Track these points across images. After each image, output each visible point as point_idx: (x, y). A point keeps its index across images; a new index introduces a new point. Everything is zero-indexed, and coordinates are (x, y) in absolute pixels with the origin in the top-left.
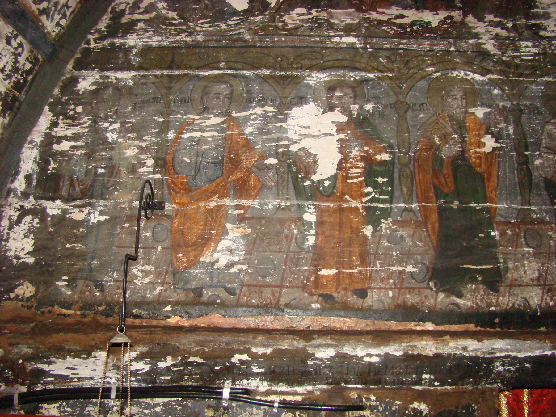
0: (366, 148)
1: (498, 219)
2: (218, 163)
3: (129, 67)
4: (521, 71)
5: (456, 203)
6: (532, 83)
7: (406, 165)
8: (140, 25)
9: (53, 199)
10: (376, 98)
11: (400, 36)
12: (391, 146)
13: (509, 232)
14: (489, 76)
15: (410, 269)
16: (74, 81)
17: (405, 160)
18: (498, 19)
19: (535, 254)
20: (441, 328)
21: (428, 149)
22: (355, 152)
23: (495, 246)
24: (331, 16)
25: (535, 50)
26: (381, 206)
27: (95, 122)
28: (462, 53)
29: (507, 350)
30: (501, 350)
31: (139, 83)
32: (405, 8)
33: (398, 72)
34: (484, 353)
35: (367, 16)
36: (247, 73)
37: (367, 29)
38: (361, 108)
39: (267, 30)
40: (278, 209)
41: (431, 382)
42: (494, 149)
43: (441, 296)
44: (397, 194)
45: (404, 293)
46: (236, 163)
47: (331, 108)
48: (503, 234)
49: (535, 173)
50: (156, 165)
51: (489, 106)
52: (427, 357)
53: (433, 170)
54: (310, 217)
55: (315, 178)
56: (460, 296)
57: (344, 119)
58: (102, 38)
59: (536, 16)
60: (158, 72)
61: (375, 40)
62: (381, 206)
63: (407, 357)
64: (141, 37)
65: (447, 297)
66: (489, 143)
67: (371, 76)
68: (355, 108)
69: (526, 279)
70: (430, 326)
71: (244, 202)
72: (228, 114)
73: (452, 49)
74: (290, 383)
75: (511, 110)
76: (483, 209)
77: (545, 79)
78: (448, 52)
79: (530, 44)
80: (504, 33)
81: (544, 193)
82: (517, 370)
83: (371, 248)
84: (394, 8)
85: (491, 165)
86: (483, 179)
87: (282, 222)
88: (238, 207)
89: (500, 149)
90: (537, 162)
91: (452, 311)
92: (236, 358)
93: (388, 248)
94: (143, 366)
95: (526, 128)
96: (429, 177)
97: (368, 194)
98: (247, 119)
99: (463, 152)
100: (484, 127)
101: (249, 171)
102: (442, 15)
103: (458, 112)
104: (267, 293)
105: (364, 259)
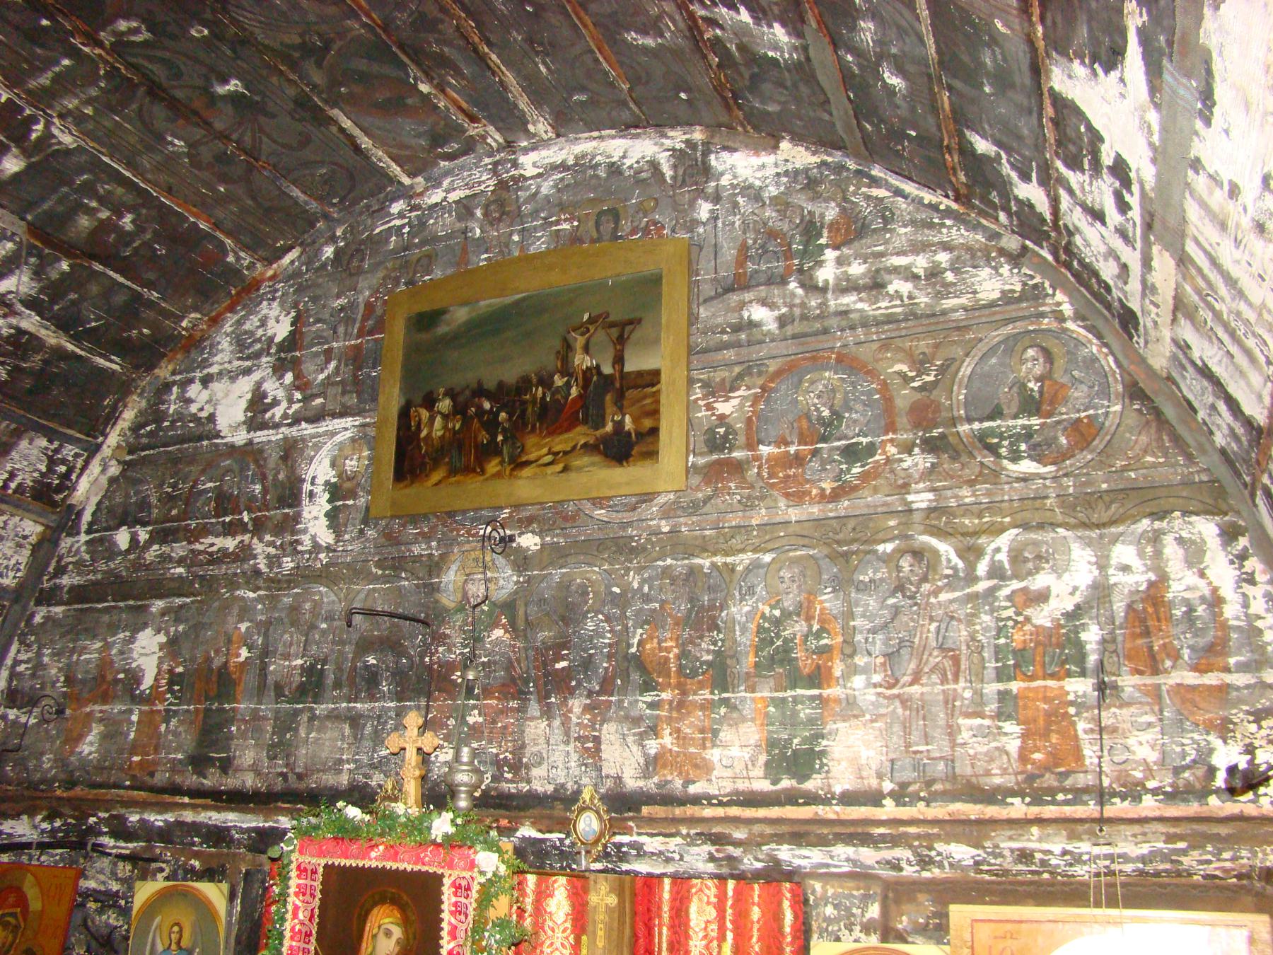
1: (239, 717)
6: (285, 595)
8: (71, 567)
9: (12, 708)
10: (187, 620)
11: (210, 562)
15: (180, 756)
16: (33, 615)
22: (165, 667)
24: (172, 550)
25: (292, 565)
27: (39, 648)
28: (244, 573)
41: (201, 844)
43: (195, 777)
46: (103, 677)
47: (158, 632)
48: (239, 729)
60: (76, 606)
66: (244, 653)
67: (188, 600)
71: (104, 708)
72: (105, 640)
74: (126, 841)
78: (236, 574)
81: (272, 694)
85: (241, 673)
88: (101, 711)
90: (272, 668)
99: (226, 663)
105: (156, 751)
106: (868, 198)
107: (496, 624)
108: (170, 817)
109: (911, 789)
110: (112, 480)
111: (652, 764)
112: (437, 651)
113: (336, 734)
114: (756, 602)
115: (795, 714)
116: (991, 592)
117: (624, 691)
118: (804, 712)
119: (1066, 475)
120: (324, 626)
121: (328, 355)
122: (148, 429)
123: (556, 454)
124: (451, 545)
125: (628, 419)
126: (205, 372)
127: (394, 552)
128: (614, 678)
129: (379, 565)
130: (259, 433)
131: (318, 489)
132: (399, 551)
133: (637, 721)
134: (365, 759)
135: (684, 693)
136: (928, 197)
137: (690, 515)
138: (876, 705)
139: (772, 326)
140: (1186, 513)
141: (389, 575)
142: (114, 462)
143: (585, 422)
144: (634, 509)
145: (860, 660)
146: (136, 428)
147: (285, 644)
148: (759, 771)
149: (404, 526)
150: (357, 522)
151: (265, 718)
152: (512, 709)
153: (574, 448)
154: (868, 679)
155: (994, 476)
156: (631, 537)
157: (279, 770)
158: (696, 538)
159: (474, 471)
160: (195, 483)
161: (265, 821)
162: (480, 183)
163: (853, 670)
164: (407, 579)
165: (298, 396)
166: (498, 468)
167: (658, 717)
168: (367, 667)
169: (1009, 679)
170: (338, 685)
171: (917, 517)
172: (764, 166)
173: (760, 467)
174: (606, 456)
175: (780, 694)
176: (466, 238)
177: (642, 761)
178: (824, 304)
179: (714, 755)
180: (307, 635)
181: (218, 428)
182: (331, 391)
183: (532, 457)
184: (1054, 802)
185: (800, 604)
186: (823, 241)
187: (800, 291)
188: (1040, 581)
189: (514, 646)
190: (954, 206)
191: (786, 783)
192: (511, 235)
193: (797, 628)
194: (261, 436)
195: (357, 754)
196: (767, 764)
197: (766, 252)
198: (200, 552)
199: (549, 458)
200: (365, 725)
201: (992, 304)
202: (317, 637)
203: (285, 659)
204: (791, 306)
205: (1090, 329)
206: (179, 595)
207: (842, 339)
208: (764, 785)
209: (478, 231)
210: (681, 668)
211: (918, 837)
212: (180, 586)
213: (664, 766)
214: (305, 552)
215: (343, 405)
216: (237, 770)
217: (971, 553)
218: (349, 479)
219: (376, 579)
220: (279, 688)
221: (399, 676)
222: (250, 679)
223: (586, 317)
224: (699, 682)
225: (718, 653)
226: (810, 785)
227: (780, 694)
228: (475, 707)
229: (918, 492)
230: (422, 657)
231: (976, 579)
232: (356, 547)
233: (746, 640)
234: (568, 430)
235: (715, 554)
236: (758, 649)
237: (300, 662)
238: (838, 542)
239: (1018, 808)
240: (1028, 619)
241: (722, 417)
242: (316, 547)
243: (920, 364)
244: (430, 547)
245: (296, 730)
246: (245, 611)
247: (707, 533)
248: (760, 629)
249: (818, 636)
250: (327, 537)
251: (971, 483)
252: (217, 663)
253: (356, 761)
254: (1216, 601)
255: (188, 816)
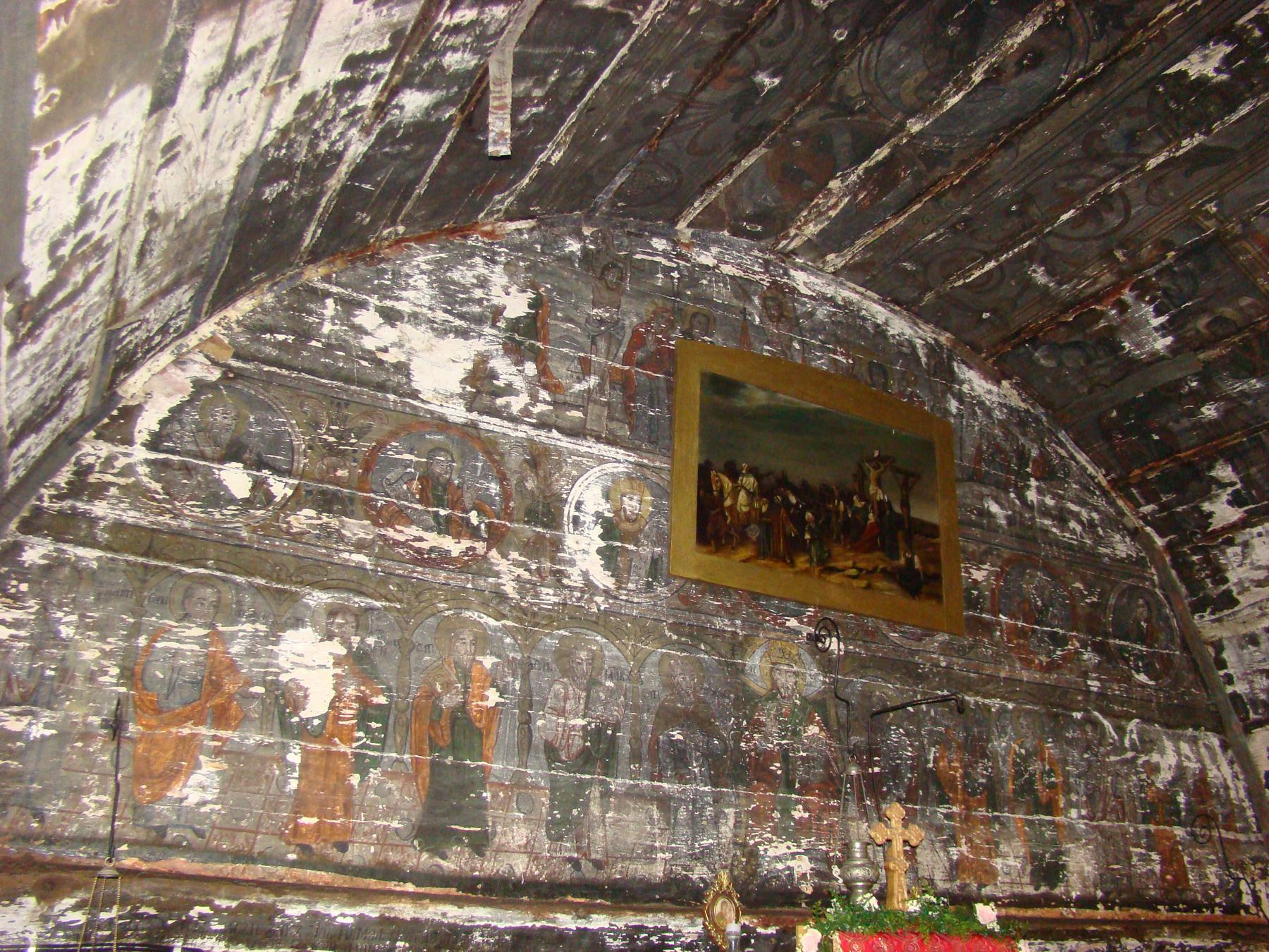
0: (363, 688)
1: (492, 779)
2: (197, 683)
3: (94, 544)
4: (537, 620)
5: (451, 758)
6: (546, 635)
7: (403, 712)
8: (113, 491)
11: (416, 562)
12: (389, 689)
13: (501, 794)
14: (504, 622)
15: (395, 824)
17: (402, 706)
18: (523, 559)
19: (525, 820)
20: (421, 890)
21: (428, 697)
22: (351, 691)
23: (486, 809)
25: (556, 599)
26: (371, 753)
27: (44, 608)
29: (487, 919)
30: (481, 919)
31: (107, 567)
32: (426, 529)
33: (408, 604)
34: (464, 921)
35: (383, 532)
36: (239, 579)
37: (381, 548)
38: (362, 641)
39: (265, 529)
40: (260, 745)
42: (497, 704)
43: (425, 856)
44: (390, 742)
45: (386, 850)
46: (217, 687)
47: (330, 637)
48: (494, 796)
49: (536, 735)
50: (121, 676)
51: (498, 656)
52: (403, 921)
53: (431, 720)
54: (294, 757)
55: (304, 714)
56: (444, 857)
57: (343, 651)
58: (60, 497)
59: (562, 561)
60: (131, 558)
61: (388, 563)
62: (371, 753)
63: (384, 920)
64: (113, 506)
65: (431, 857)
66: (493, 697)
67: (378, 604)
68: (355, 640)
69: (513, 845)
70: (410, 887)
71: (222, 733)
72: (212, 626)
73: (469, 586)
75: (521, 663)
76: (477, 767)
77: (562, 632)
79: (551, 591)
80: (526, 575)
81: (542, 756)
82: (497, 942)
83: (357, 799)
84: (414, 527)
85: (491, 721)
86: (481, 735)
87: (264, 760)
88: (215, 738)
89: (503, 704)
90: (540, 723)
91: (434, 872)
92: (195, 912)
93: (374, 800)
94: (80, 917)
95: (533, 685)
96: (425, 727)
97: (359, 739)
98: (233, 635)
99: (465, 703)
100: (490, 679)
101: (231, 697)
102: (466, 543)
103: (465, 660)
104: (241, 839)
105: (348, 809)
106: (1056, 452)
107: (811, 721)
108: (371, 911)
109: (1112, 896)
110: (200, 386)
111: (956, 868)
112: (753, 738)
113: (642, 816)
114: (1010, 739)
115: (1042, 833)
116: (1134, 759)
117: (924, 801)
118: (1048, 834)
119: (1161, 689)
120: (609, 684)
121: (586, 367)
122: (281, 337)
123: (860, 570)
124: (757, 628)
125: (916, 559)
126: (389, 303)
127: (692, 619)
128: (916, 788)
129: (673, 626)
130: (486, 418)
131: (588, 519)
132: (699, 619)
133: (939, 829)
134: (684, 849)
135: (968, 808)
136: (1090, 470)
137: (959, 657)
138: (1086, 831)
139: (1003, 522)
140: (1207, 730)
141: (686, 643)
142: (200, 358)
143: (882, 549)
144: (920, 640)
145: (1074, 797)
146: (255, 328)
147: (556, 696)
148: (1026, 879)
149: (703, 592)
150: (643, 572)
151: (535, 786)
152: (834, 808)
153: (875, 569)
154: (1079, 812)
155: (1129, 679)
156: (918, 665)
157: (567, 855)
158: (964, 677)
159: (784, 561)
160: (381, 446)
161: (535, 920)
162: (754, 272)
163: (1070, 804)
164: (706, 652)
165: (544, 395)
166: (807, 565)
167: (954, 828)
168: (672, 743)
169: (1150, 823)
170: (635, 757)
171: (1093, 697)
172: (990, 392)
173: (1001, 631)
174: (900, 585)
175: (1030, 817)
176: (745, 319)
177: (947, 865)
178: (1032, 519)
179: (998, 863)
180: (588, 690)
181: (415, 385)
182: (593, 409)
183: (839, 565)
184: (1179, 910)
185: (1035, 747)
186: (1029, 470)
187: (1017, 502)
188: (1155, 757)
189: (830, 745)
190: (1104, 483)
191: (1043, 889)
192: (792, 339)
193: (1035, 766)
194: (489, 424)
195: (673, 841)
196: (1032, 873)
197: (994, 460)
198: (397, 543)
199: (853, 572)
200: (677, 810)
201: (1122, 560)
202: (603, 697)
203: (559, 715)
204: (1014, 512)
205: (1167, 597)
206: (361, 593)
207: (1045, 551)
208: (1030, 890)
209: (757, 319)
210: (965, 786)
211: (1112, 933)
212: (356, 581)
213: (963, 872)
214: (576, 588)
215: (611, 432)
216: (500, 850)
217: (1121, 731)
218: (628, 520)
219: (669, 643)
220: (551, 752)
221: (709, 757)
222: (507, 731)
223: (876, 454)
224: (979, 800)
225: (989, 778)
226: (1059, 890)
227: (1030, 817)
228: (798, 802)
229: (1093, 679)
230: (737, 742)
231: (1125, 750)
232: (644, 600)
233: (1007, 770)
234: (868, 551)
235: (977, 694)
236: (1015, 779)
237: (580, 722)
238: (1052, 705)
239: (1163, 912)
240: (1153, 783)
241: (975, 581)
242: (589, 587)
243: (1089, 586)
244: (733, 625)
245: (586, 806)
246: (483, 641)
247: (972, 675)
248: (1015, 764)
249: (1050, 776)
250: (603, 579)
251: (1119, 682)
252: (449, 701)
253: (672, 850)
254: (1227, 788)
255: (406, 911)
